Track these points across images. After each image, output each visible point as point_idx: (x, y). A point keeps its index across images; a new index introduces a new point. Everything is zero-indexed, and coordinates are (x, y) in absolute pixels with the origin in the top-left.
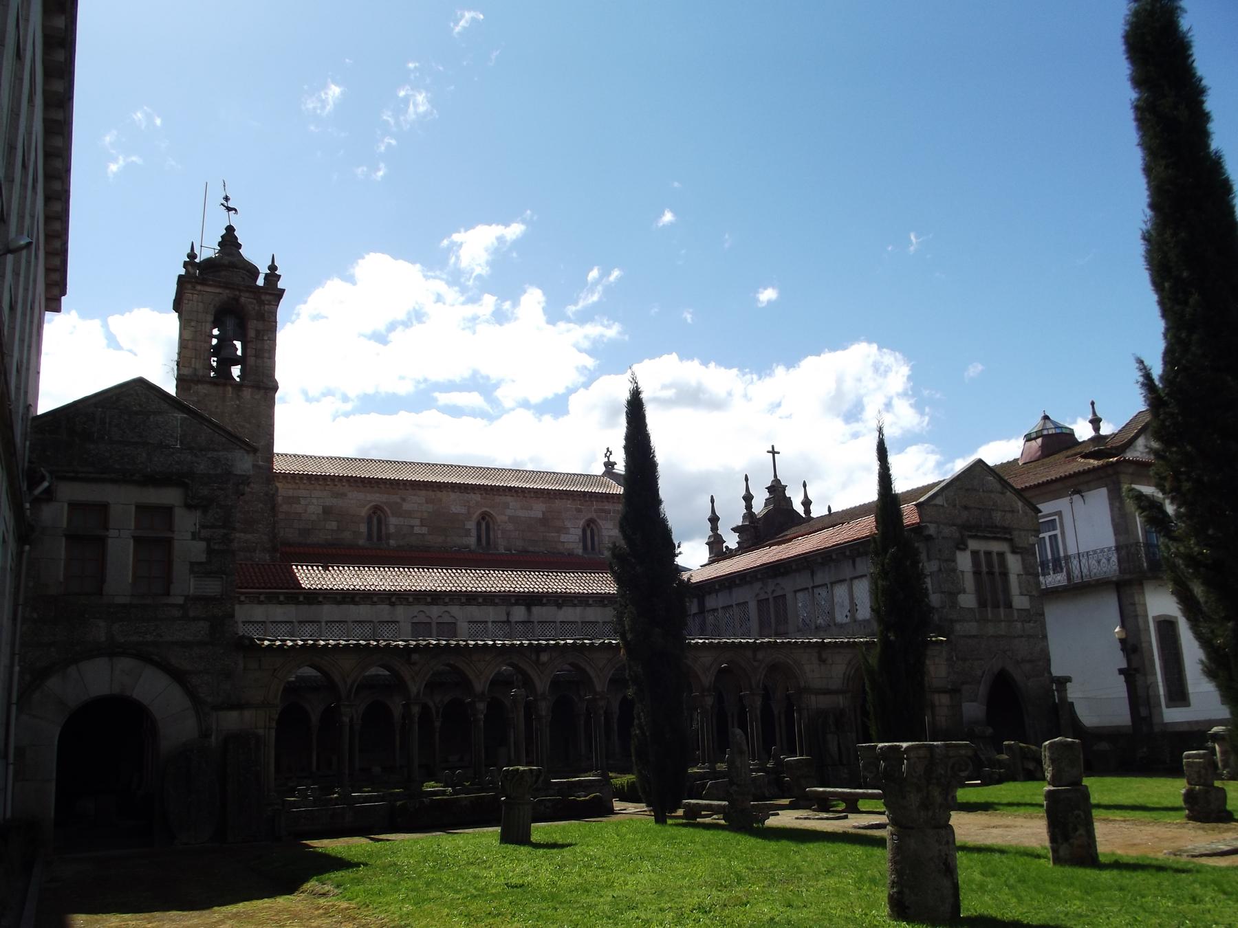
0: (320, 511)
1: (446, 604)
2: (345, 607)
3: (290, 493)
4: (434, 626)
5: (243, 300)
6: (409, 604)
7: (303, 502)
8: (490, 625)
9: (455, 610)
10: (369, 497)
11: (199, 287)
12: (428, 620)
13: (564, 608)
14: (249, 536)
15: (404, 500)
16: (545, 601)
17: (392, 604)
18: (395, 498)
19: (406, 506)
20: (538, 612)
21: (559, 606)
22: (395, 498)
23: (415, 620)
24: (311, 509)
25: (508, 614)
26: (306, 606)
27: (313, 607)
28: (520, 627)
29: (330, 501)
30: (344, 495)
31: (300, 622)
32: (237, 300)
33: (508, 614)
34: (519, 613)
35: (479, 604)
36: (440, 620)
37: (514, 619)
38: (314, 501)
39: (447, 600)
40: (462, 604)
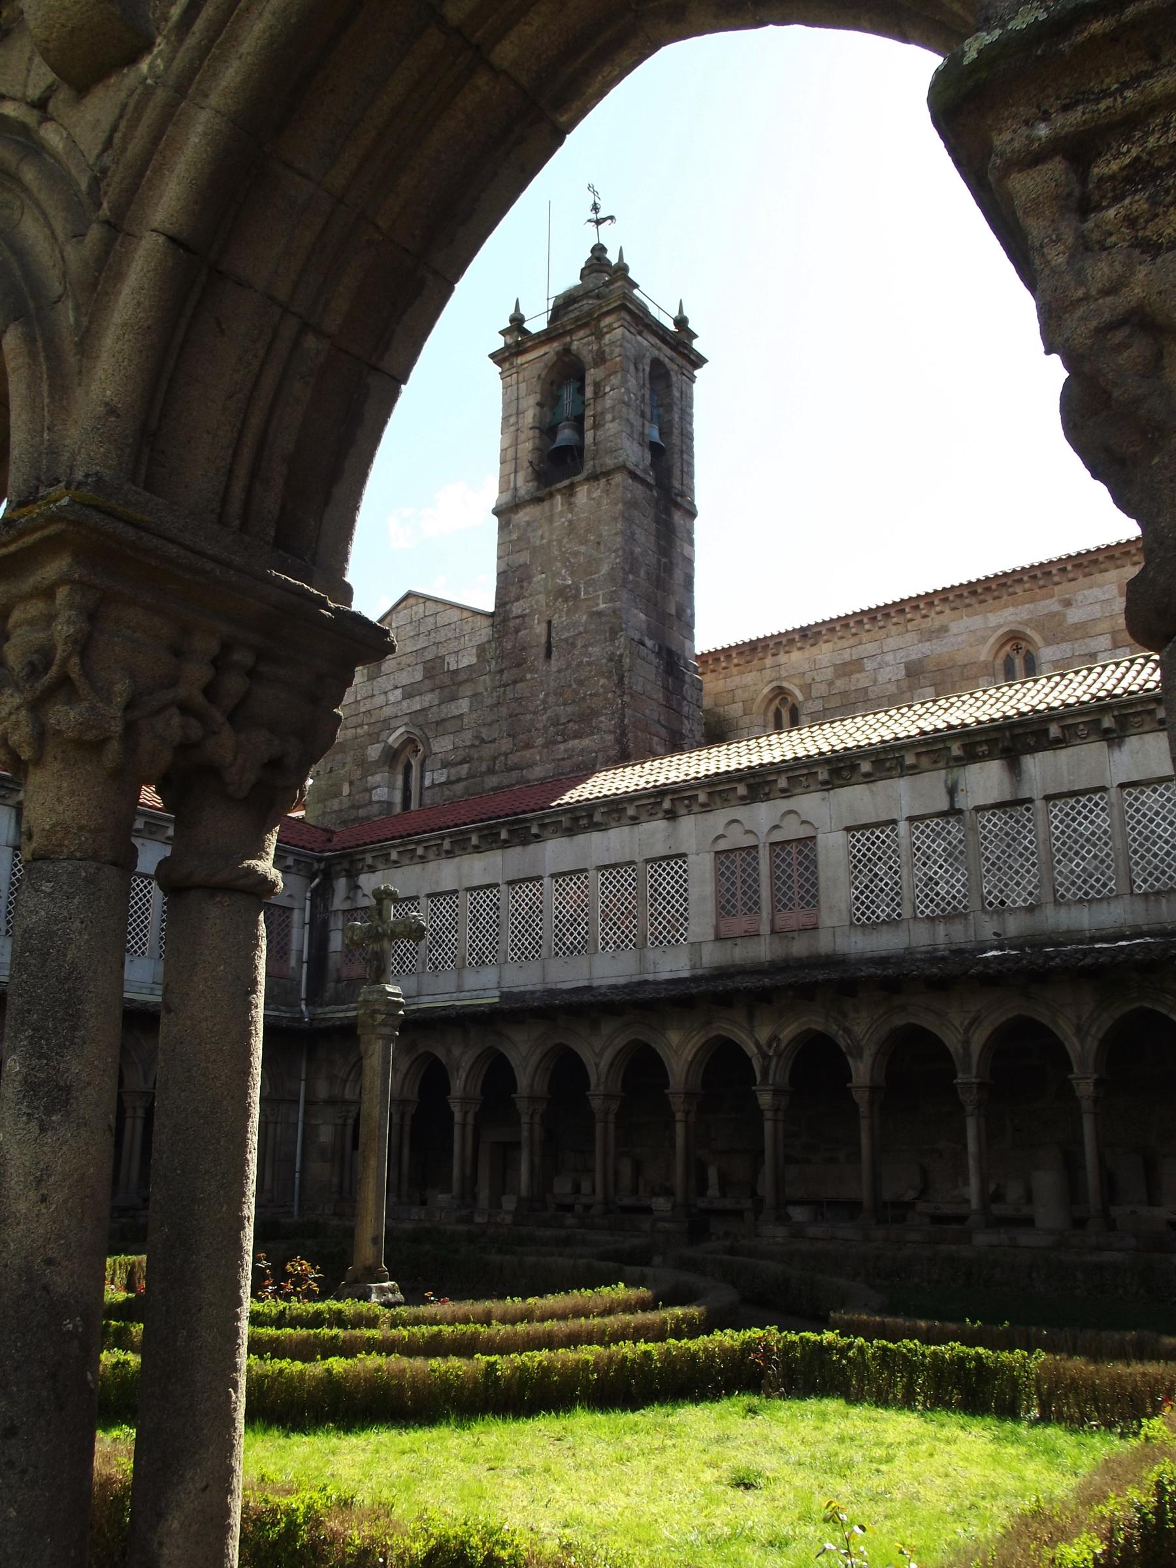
0: (902, 673)
1: (786, 793)
2: (581, 839)
3: (847, 656)
4: (764, 855)
5: (575, 346)
6: (706, 808)
7: (869, 665)
8: (903, 827)
9: (811, 805)
10: (993, 619)
11: (520, 360)
12: (748, 841)
13: (1132, 743)
14: (586, 742)
15: (1068, 603)
16: (1054, 730)
17: (671, 816)
18: (1053, 605)
19: (1074, 616)
20: (1042, 770)
21: (1113, 738)
22: (1053, 605)
23: (723, 845)
24: (885, 675)
25: (952, 791)
26: (519, 849)
27: (531, 847)
28: (994, 822)
29: (918, 650)
30: (944, 629)
31: (510, 883)
32: (567, 350)
33: (952, 791)
34: (985, 781)
35: (869, 779)
36: (778, 836)
37: (965, 802)
38: (889, 658)
39: (783, 783)
40: (826, 786)
